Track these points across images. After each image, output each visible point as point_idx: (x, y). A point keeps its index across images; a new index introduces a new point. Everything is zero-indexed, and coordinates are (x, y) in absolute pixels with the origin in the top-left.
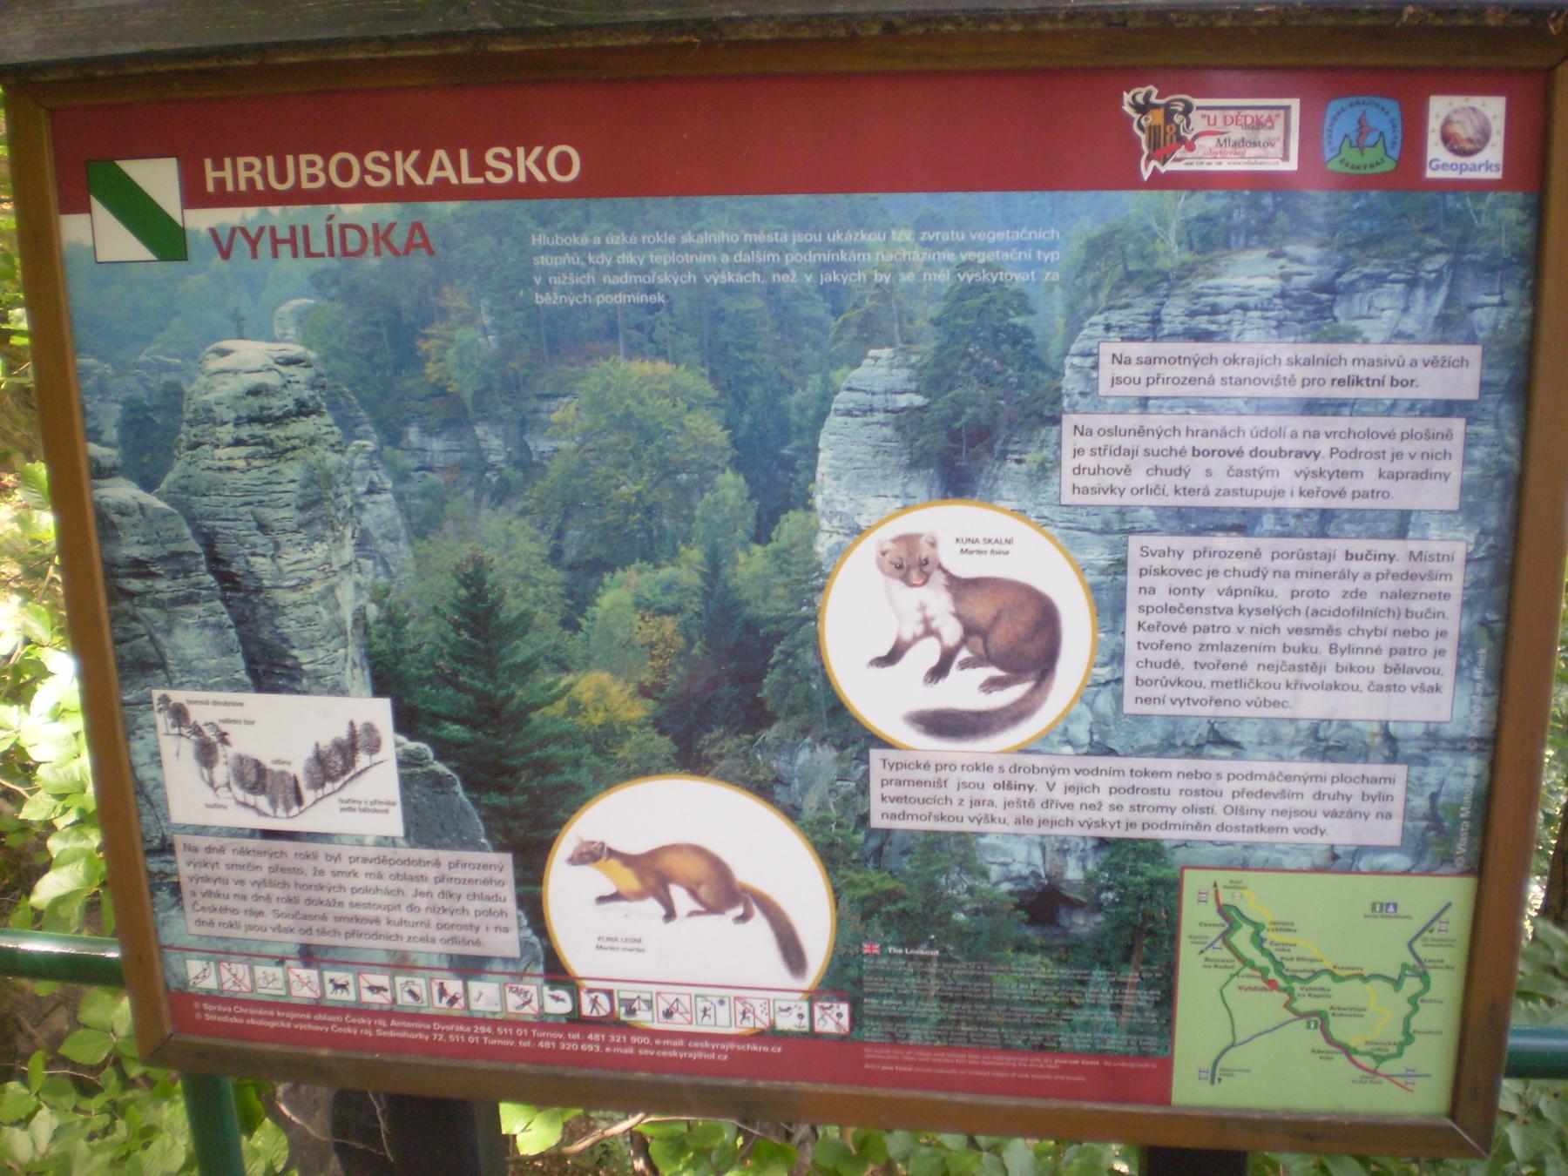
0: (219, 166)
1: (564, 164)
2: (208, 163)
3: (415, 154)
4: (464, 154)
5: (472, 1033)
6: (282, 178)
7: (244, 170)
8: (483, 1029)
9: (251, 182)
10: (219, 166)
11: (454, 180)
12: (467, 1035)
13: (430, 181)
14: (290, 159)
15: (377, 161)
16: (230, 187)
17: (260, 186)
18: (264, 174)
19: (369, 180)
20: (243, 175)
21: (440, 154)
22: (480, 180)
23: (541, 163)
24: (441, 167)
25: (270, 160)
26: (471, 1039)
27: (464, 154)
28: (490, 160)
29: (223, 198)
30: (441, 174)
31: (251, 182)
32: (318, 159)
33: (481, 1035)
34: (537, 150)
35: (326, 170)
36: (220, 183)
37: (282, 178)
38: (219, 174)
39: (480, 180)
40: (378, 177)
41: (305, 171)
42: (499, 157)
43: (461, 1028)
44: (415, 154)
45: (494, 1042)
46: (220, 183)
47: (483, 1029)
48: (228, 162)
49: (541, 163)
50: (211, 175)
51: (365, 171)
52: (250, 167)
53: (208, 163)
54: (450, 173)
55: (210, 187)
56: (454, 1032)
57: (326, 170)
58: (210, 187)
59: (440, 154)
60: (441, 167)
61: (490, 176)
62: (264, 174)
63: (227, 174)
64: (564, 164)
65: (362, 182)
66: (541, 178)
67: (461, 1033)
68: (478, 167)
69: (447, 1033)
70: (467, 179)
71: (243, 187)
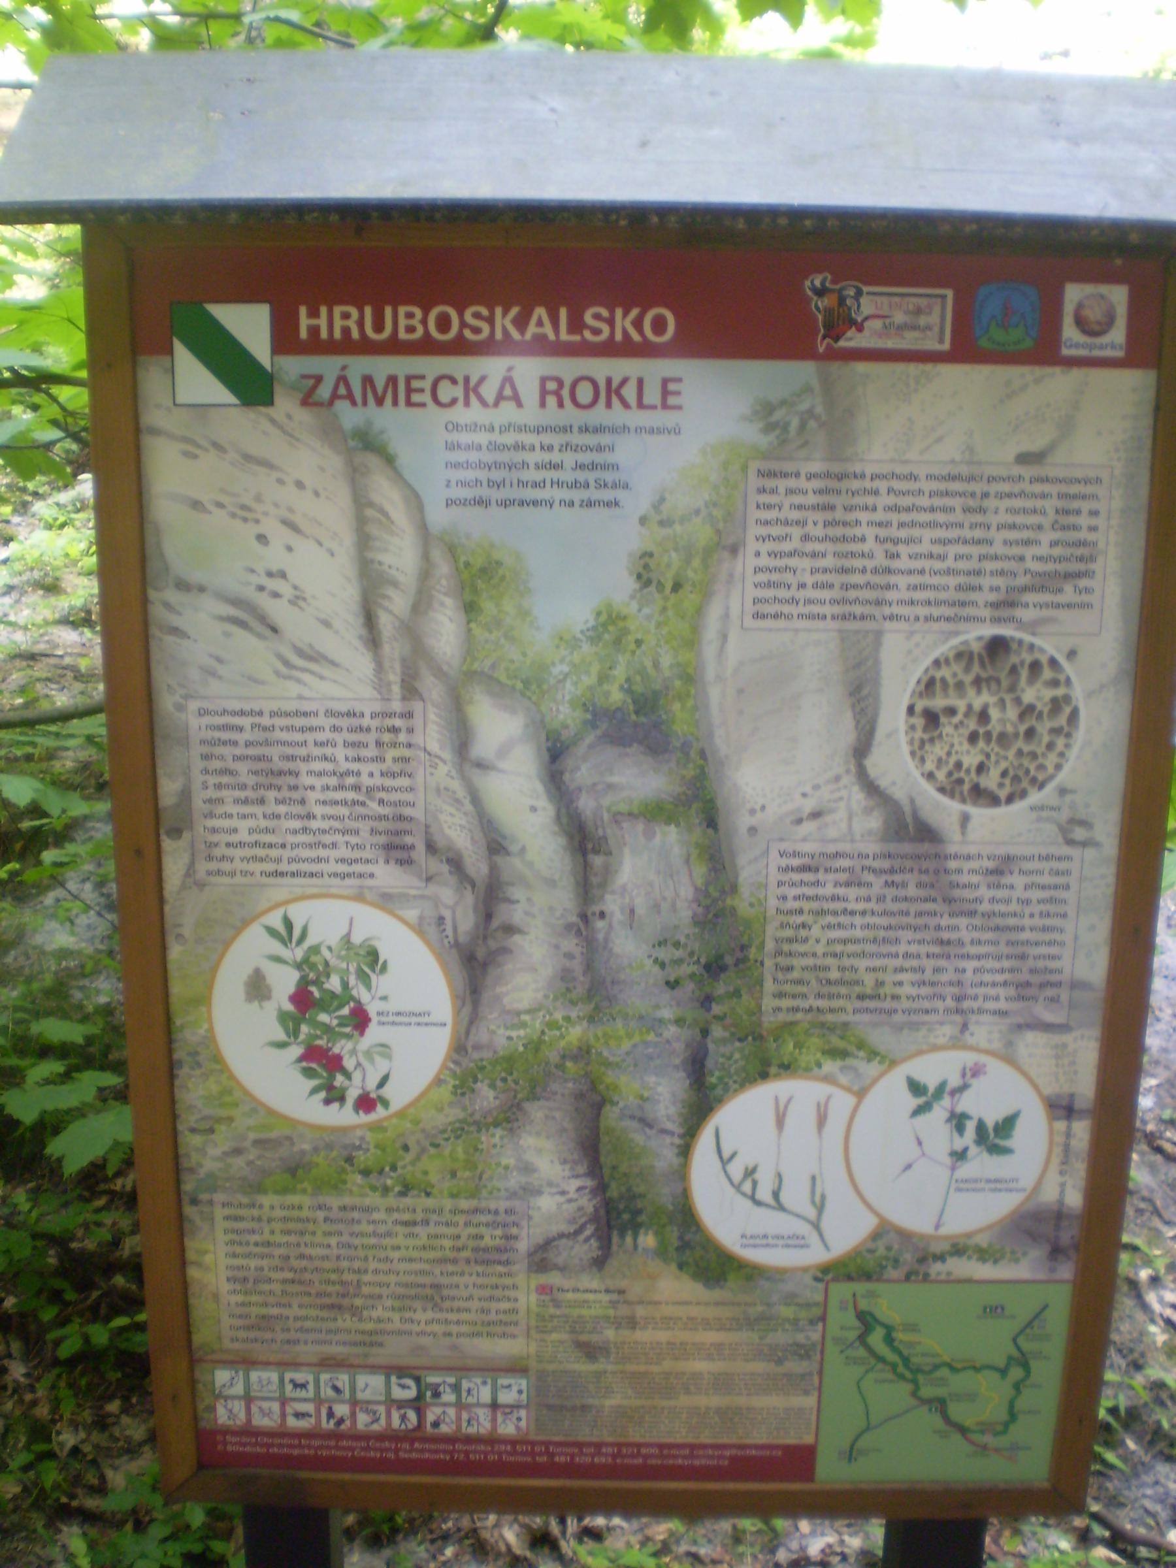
0: (314, 313)
1: (659, 325)
2: (303, 311)
3: (515, 311)
4: (563, 313)
5: (492, 1452)
6: (379, 326)
7: (341, 319)
8: (503, 1447)
9: (346, 331)
10: (314, 313)
11: (552, 336)
12: (486, 1454)
13: (528, 336)
14: (388, 311)
15: (477, 316)
16: (324, 334)
17: (355, 334)
18: (361, 324)
19: (468, 333)
20: (338, 323)
21: (540, 312)
22: (576, 338)
23: (638, 324)
24: (540, 323)
25: (368, 311)
26: (491, 1458)
27: (563, 313)
28: (588, 318)
29: (316, 346)
30: (539, 330)
31: (346, 331)
32: (418, 313)
33: (500, 1454)
34: (635, 312)
35: (424, 322)
36: (314, 331)
37: (379, 326)
38: (314, 322)
39: (576, 338)
40: (476, 331)
41: (403, 322)
42: (597, 317)
43: (482, 1447)
44: (515, 311)
45: (512, 1459)
46: (314, 331)
47: (503, 1447)
48: (324, 310)
49: (638, 324)
50: (304, 322)
51: (463, 324)
52: (346, 316)
53: (303, 311)
54: (548, 330)
55: (303, 334)
56: (475, 1452)
57: (424, 322)
58: (303, 334)
59: (540, 312)
60: (540, 323)
61: (587, 334)
62: (361, 324)
63: (323, 322)
64: (659, 325)
65: (460, 335)
66: (636, 337)
67: (480, 1452)
68: (576, 325)
69: (467, 1453)
70: (564, 336)
71: (337, 334)
